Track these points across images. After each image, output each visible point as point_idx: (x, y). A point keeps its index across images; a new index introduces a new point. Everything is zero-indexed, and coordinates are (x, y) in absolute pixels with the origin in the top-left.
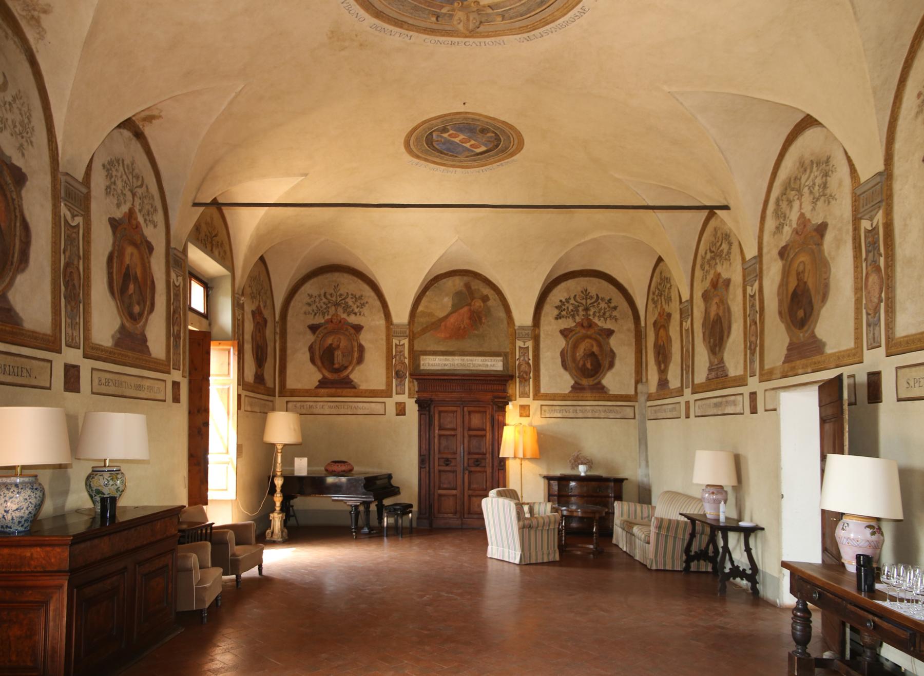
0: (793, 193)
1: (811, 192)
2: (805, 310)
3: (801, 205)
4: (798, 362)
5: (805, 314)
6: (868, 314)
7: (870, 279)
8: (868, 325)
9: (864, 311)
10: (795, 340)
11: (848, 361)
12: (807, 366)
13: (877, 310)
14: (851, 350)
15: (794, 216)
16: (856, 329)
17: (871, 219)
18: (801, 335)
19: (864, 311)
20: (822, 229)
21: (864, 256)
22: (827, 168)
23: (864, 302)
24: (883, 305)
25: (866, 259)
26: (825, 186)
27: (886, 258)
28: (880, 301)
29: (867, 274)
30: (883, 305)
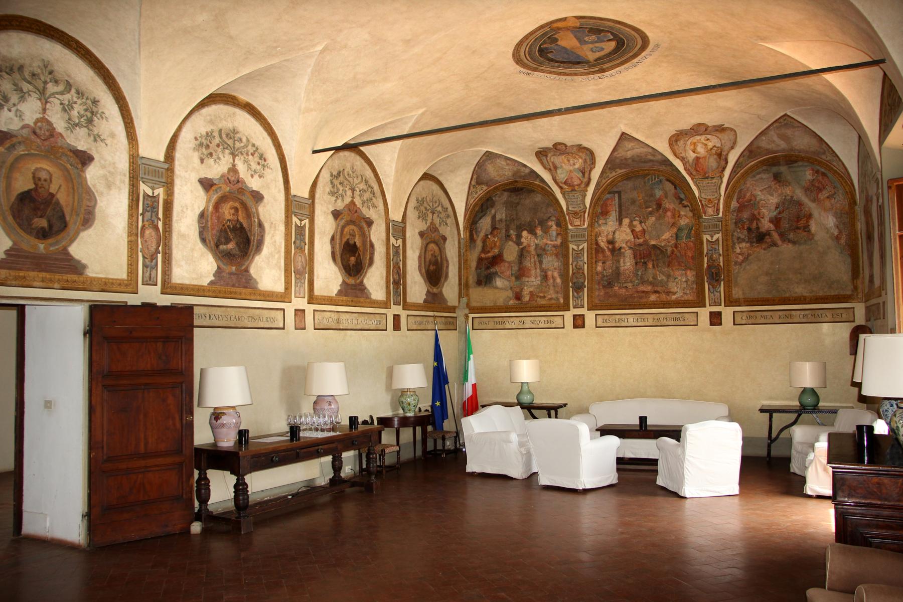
0: (31, 87)
1: (64, 110)
2: (49, 221)
3: (44, 110)
4: (32, 274)
5: (51, 226)
6: (144, 257)
7: (147, 232)
8: (145, 266)
9: (140, 254)
10: (25, 246)
11: (118, 289)
12: (51, 281)
13: (153, 257)
14: (123, 280)
15: (30, 110)
16: (130, 265)
17: (153, 189)
18: (42, 246)
19: (140, 254)
20: (85, 159)
21: (141, 211)
22: (95, 109)
23: (140, 246)
24: (160, 256)
25: (142, 214)
26: (90, 121)
27: (164, 224)
28: (157, 252)
29: (143, 226)
30: (160, 256)
